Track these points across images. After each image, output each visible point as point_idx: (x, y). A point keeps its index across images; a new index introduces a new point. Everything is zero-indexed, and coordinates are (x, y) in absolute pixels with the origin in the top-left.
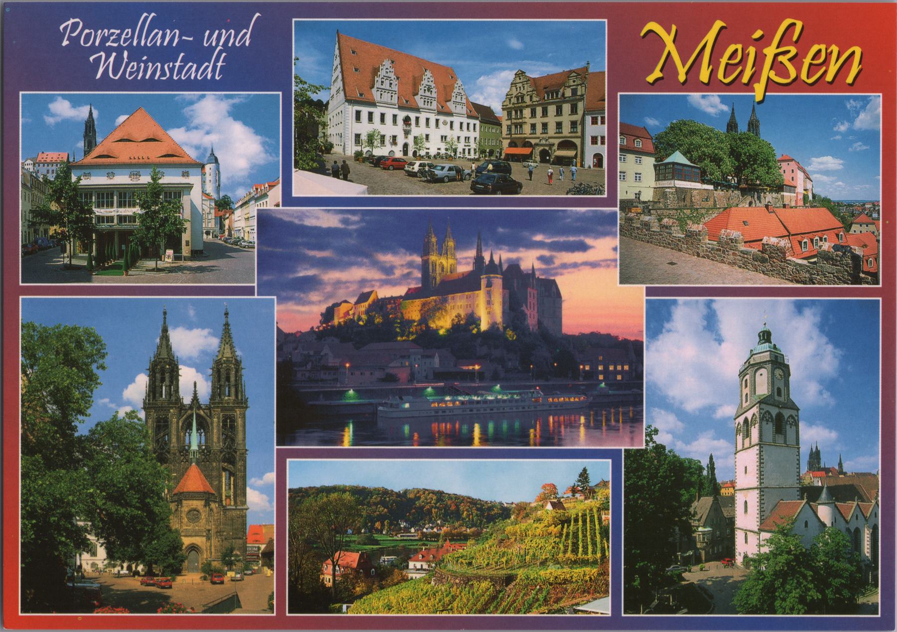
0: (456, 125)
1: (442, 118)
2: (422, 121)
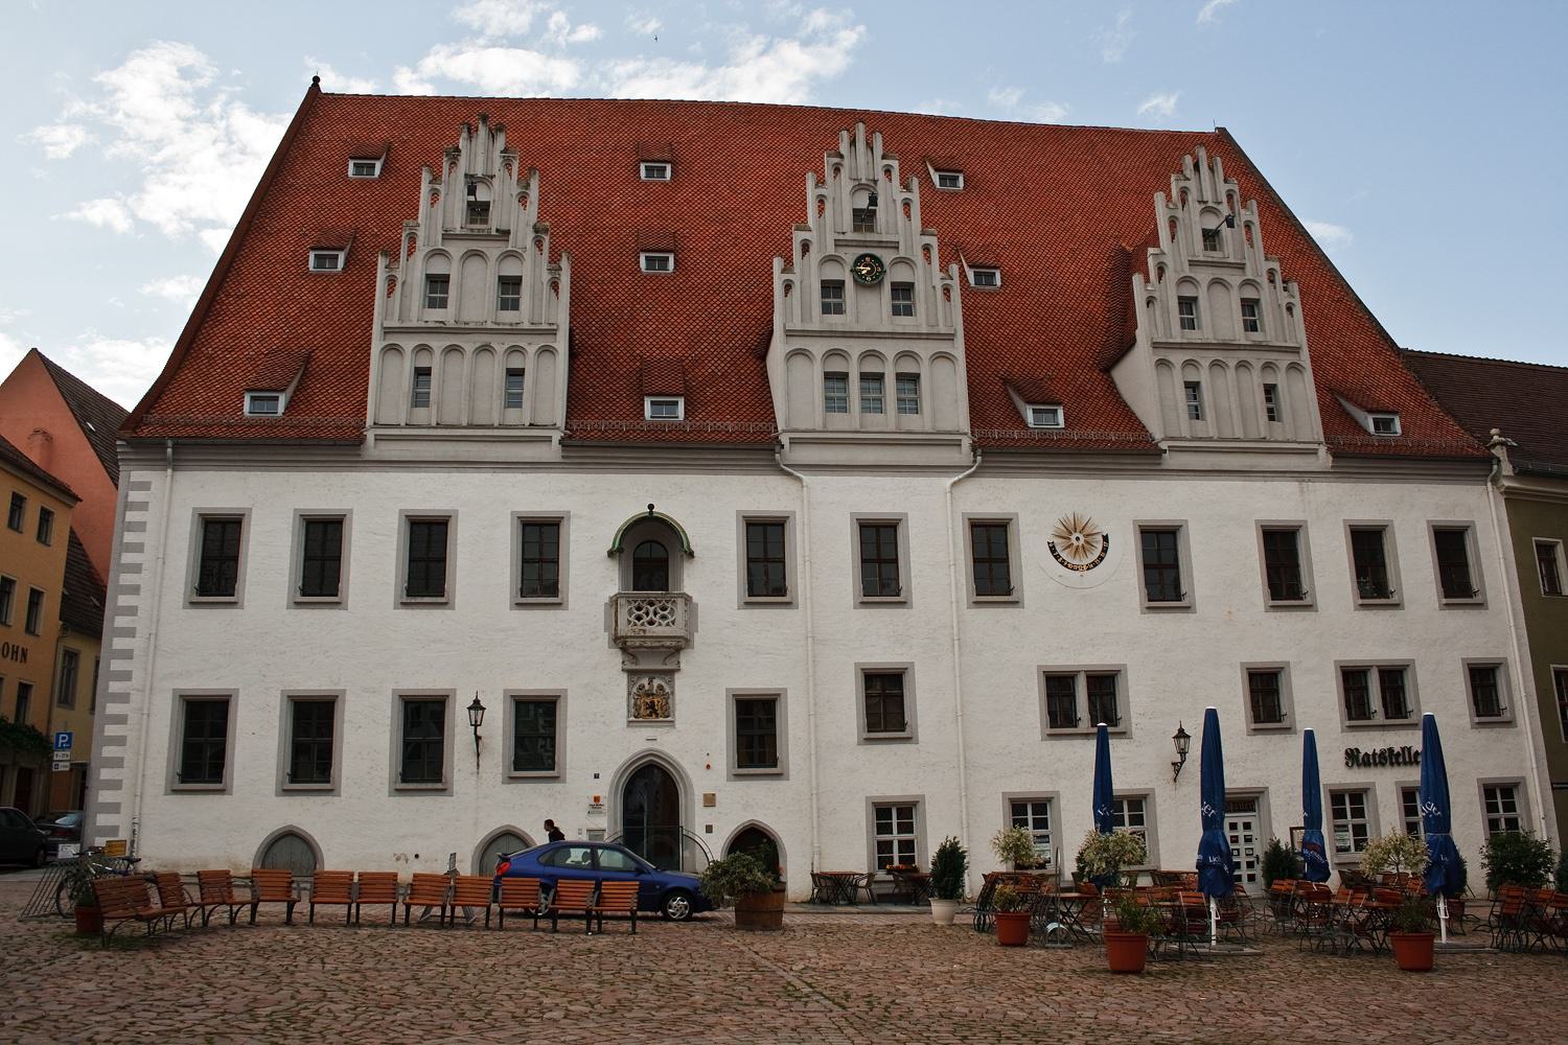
0: (1224, 562)
2: (824, 559)
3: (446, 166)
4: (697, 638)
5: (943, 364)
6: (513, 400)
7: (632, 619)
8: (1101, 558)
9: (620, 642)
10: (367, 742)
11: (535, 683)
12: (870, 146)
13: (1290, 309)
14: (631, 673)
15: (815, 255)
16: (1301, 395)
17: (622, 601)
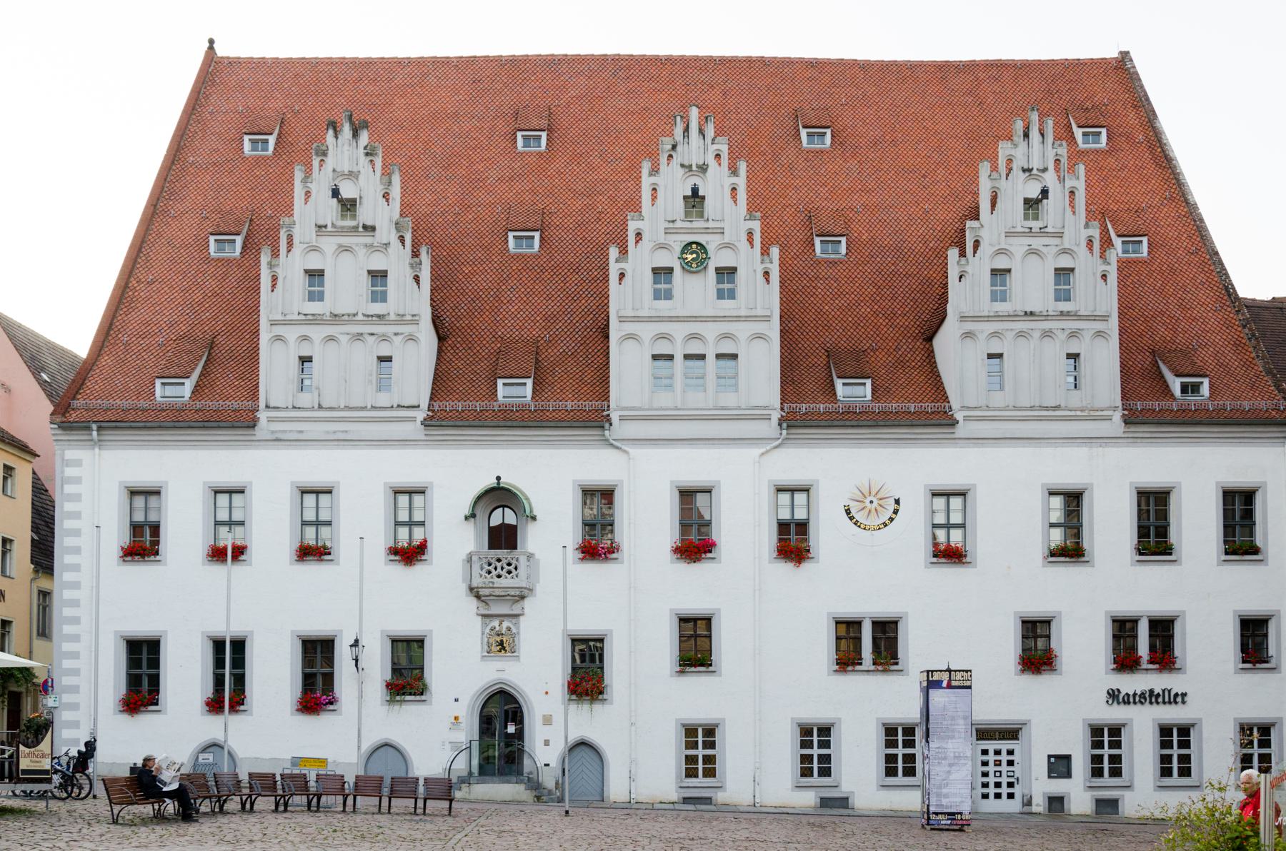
1: (838, 469)
3: (316, 162)
4: (539, 589)
5: (759, 343)
6: (383, 385)
7: (483, 573)
8: (891, 519)
9: (475, 592)
10: (274, 674)
11: (407, 628)
12: (701, 132)
13: (1104, 277)
14: (484, 616)
15: (646, 243)
16: (1104, 362)
17: (475, 558)
